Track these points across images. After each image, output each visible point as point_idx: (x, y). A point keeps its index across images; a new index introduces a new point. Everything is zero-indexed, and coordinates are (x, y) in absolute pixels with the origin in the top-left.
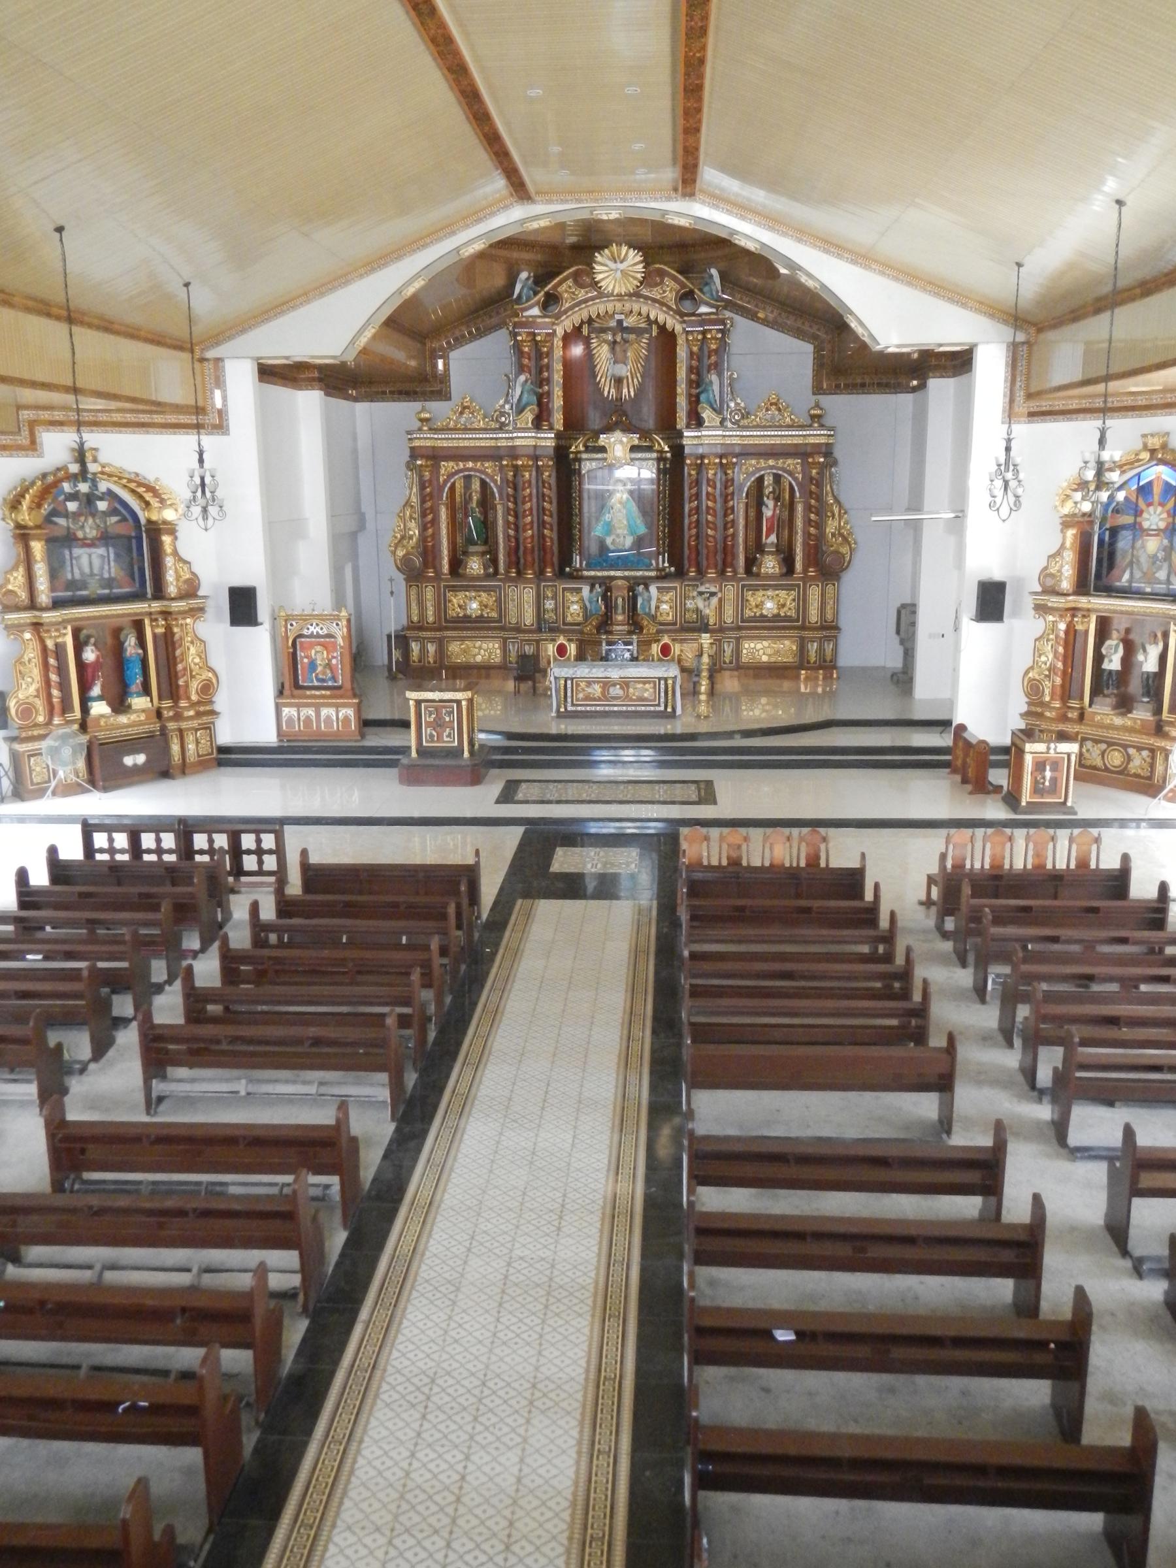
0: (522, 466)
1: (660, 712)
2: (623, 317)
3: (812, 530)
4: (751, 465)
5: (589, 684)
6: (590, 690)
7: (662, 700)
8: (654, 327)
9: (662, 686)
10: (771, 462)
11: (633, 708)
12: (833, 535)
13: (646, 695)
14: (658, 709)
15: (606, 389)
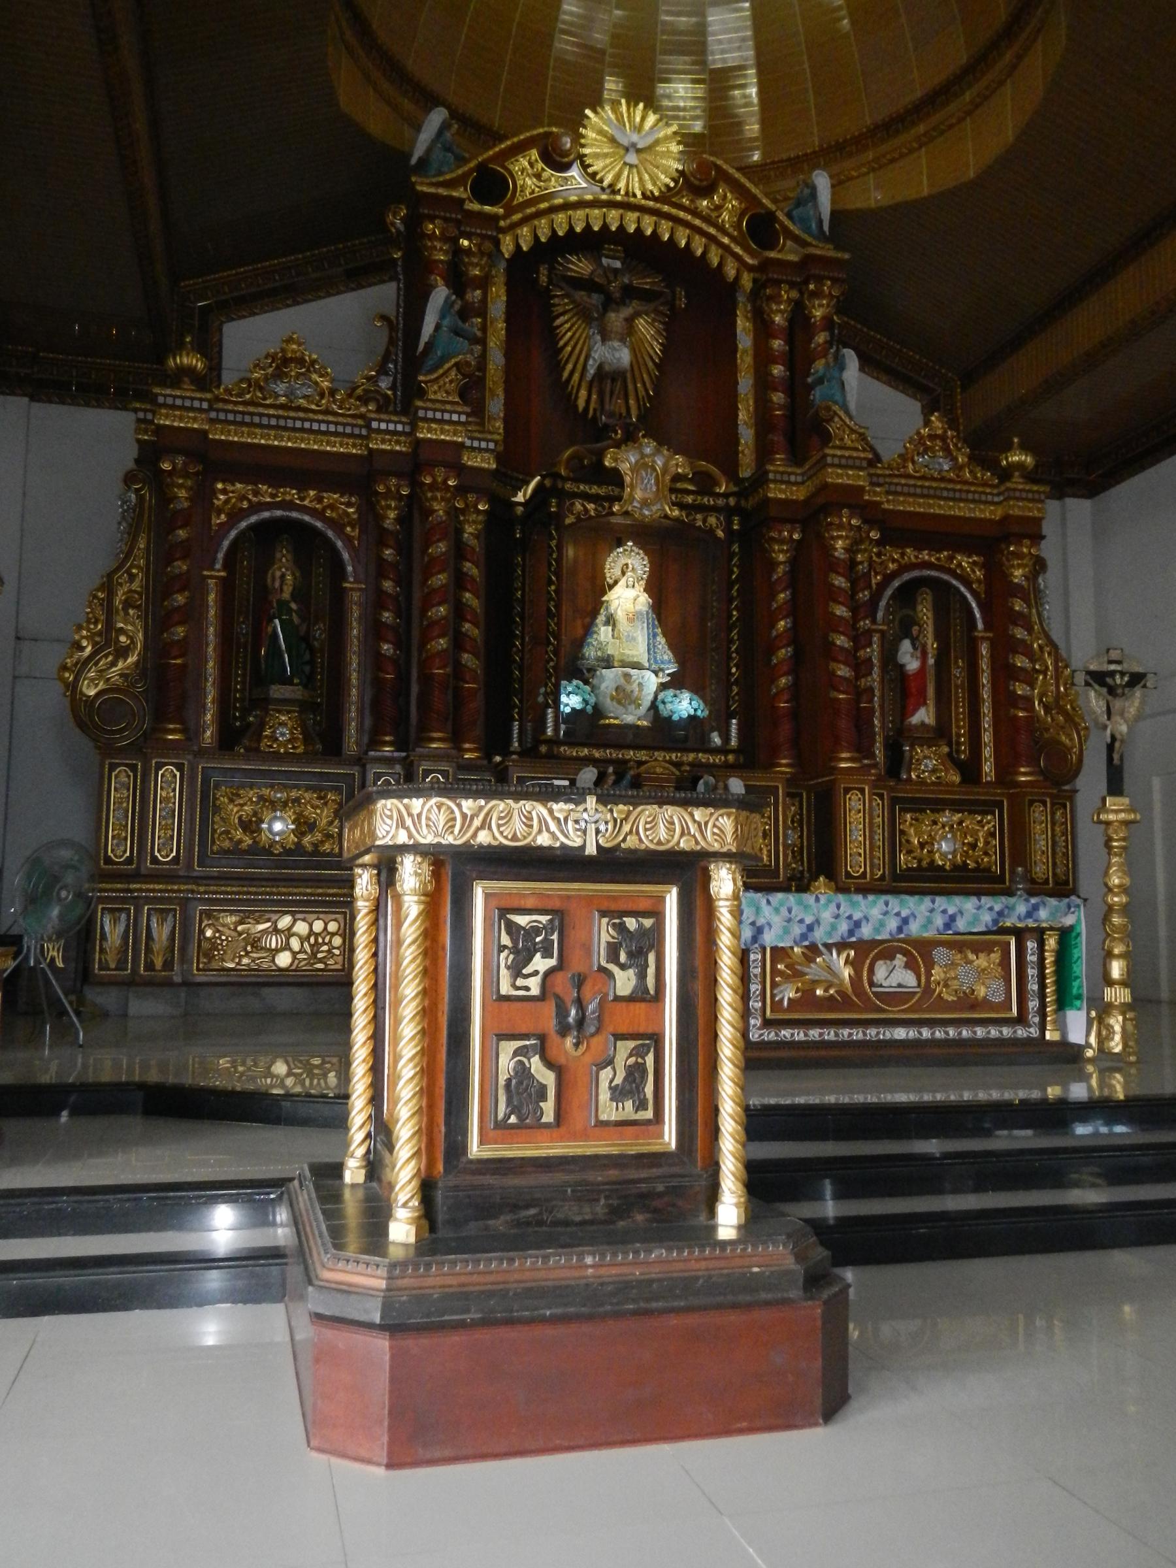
0: (433, 487)
1: (1029, 1041)
2: (618, 264)
3: (1020, 689)
4: (894, 560)
5: (813, 951)
6: (813, 971)
7: (1033, 1004)
8: (681, 293)
9: (1032, 958)
10: (925, 556)
11: (952, 1032)
12: (1047, 709)
13: (981, 991)
14: (1021, 1032)
15: (583, 393)
